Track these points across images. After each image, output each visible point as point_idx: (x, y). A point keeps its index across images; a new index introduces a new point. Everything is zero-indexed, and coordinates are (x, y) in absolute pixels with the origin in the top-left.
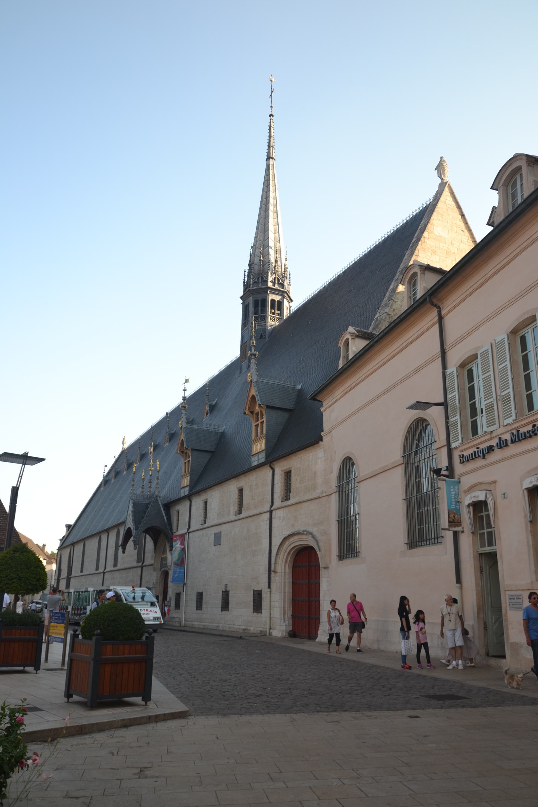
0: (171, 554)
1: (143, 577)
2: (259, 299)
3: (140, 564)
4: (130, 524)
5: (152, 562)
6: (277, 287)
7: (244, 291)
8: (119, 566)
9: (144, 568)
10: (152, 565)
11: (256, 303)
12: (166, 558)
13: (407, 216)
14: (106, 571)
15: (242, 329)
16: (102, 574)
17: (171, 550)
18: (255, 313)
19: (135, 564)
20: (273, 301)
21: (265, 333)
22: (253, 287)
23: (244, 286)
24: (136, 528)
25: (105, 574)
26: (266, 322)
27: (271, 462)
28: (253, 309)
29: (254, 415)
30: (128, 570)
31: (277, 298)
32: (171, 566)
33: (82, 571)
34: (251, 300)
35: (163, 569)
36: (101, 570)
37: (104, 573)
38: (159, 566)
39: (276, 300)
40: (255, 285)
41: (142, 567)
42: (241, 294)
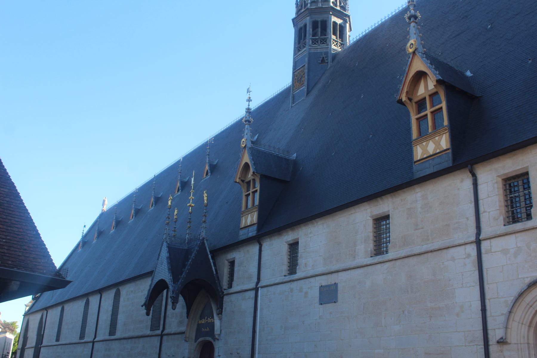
0: (220, 319)
1: (163, 349)
2: (319, 20)
3: (159, 332)
4: (163, 272)
5: (183, 329)
6: (338, 8)
7: (297, 13)
8: (118, 335)
9: (165, 338)
10: (184, 333)
11: (315, 25)
12: (212, 325)
13: (386, 16)
14: (95, 340)
15: (294, 56)
16: (91, 344)
17: (220, 313)
18: (314, 34)
19: (148, 332)
20: (335, 23)
21: (327, 57)
22: (311, 6)
23: (297, 7)
24: (175, 280)
25: (95, 344)
26: (328, 45)
27: (472, 165)
28: (311, 30)
29: (414, 104)
30: (137, 340)
31: (339, 21)
32: (219, 335)
33: (58, 340)
34: (308, 20)
35: (200, 339)
36: (89, 337)
37: (93, 342)
38: (194, 335)
39: (338, 23)
40: (314, 4)
41: (162, 336)
42: (294, 16)
